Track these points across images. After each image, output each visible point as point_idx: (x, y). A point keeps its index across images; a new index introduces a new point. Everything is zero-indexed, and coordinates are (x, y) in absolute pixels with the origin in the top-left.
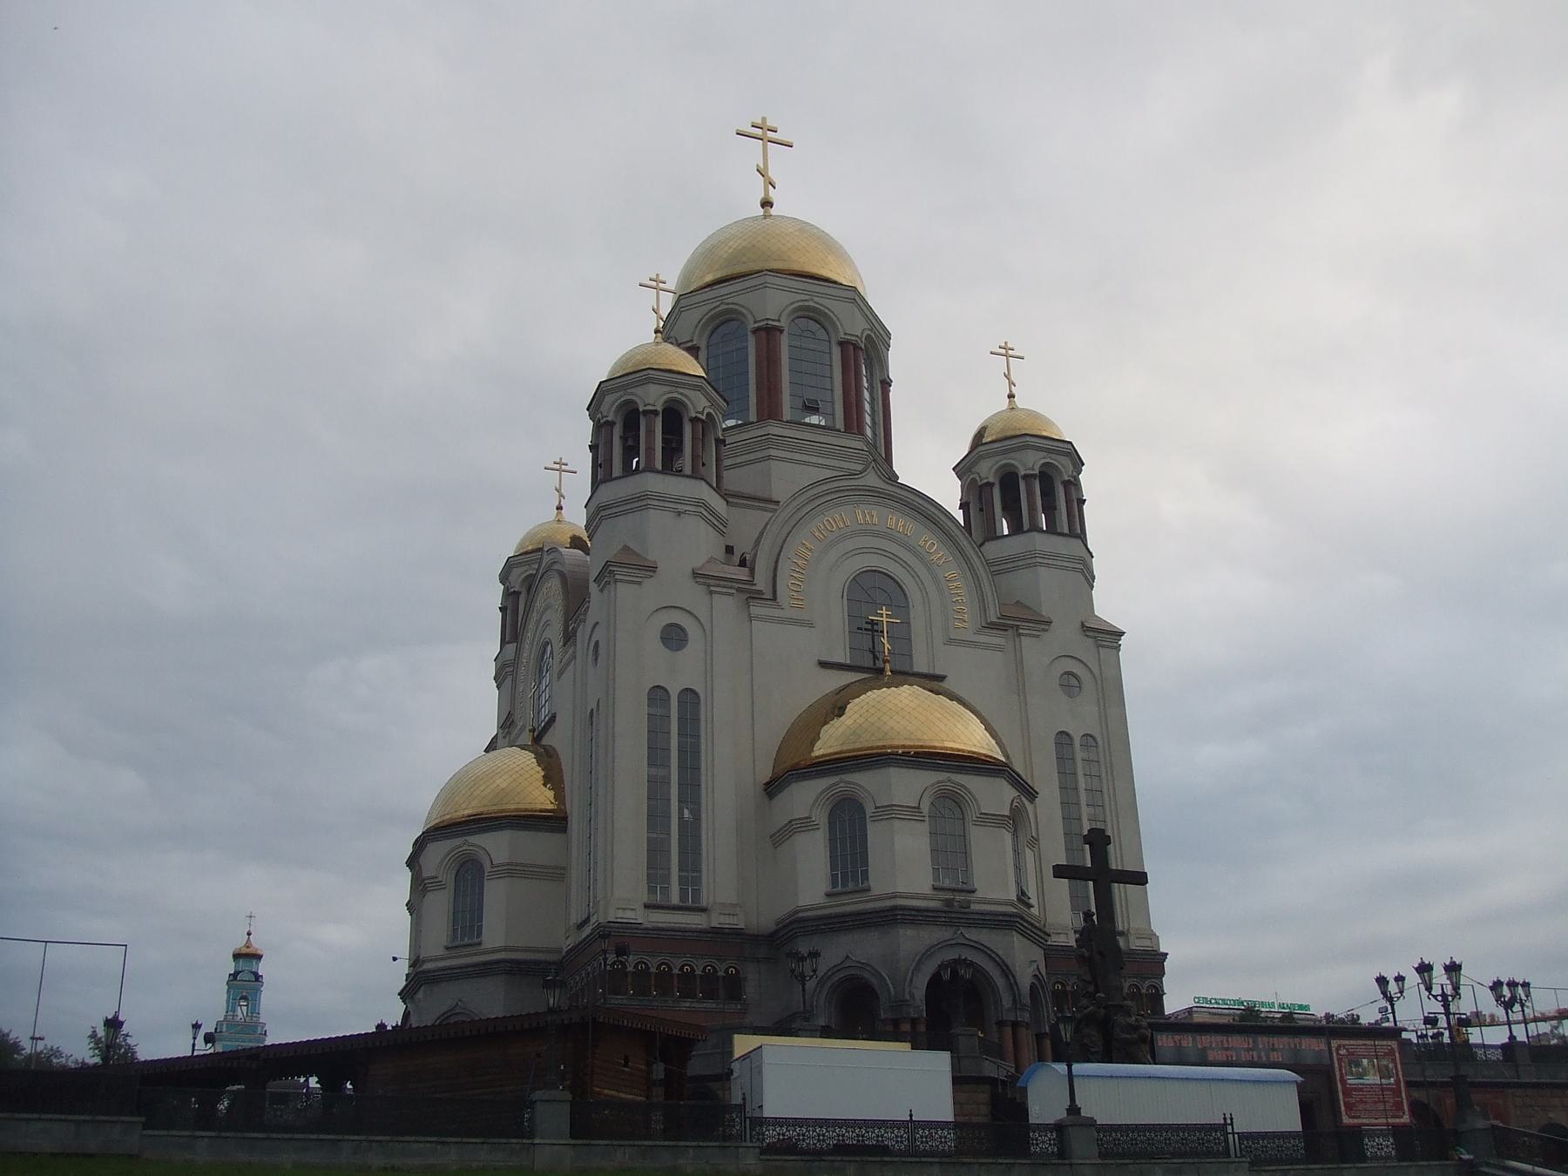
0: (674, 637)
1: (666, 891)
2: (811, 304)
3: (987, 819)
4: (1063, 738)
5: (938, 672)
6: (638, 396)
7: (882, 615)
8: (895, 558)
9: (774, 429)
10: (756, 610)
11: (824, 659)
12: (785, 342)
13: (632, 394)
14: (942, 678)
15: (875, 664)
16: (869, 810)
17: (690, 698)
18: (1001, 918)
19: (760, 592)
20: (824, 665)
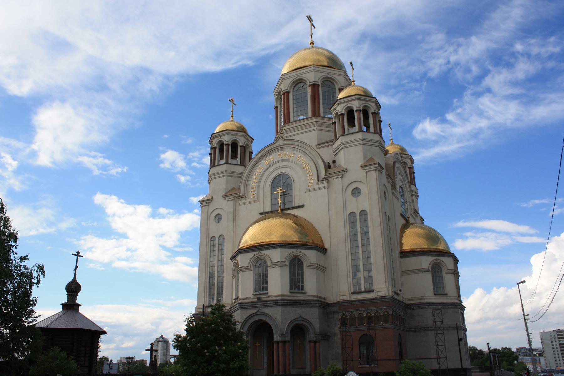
0: (218, 217)
1: (213, 300)
2: (298, 78)
3: (274, 264)
5: (301, 204)
6: (223, 139)
7: (278, 190)
8: (275, 170)
11: (262, 211)
12: (291, 95)
13: (222, 138)
14: (302, 206)
15: (284, 207)
16: (269, 263)
17: (221, 237)
19: (242, 196)
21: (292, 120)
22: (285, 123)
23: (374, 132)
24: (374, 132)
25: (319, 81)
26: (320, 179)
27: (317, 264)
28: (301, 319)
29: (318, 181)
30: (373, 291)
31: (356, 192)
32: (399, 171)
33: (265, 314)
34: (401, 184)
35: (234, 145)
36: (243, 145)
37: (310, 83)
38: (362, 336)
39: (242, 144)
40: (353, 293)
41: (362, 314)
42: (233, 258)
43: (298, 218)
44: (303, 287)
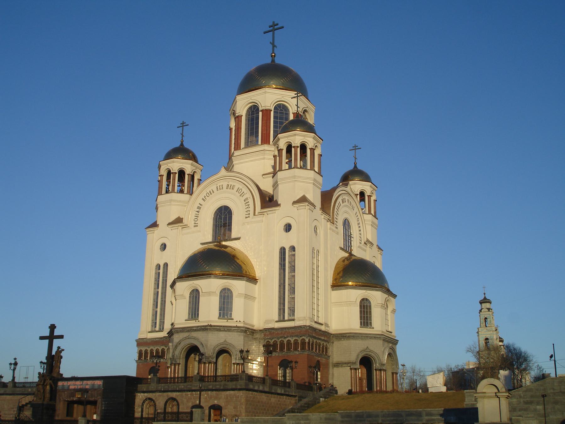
0: (164, 247)
1: (155, 327)
4: (283, 251)
5: (239, 236)
9: (237, 153)
10: (186, 231)
17: (166, 265)
18: (203, 328)
20: (202, 244)
21: (243, 145)
22: (235, 150)
23: (309, 169)
24: (309, 169)
25: (272, 106)
26: (256, 214)
27: (246, 295)
28: (225, 343)
29: (254, 215)
30: (294, 320)
31: (288, 228)
32: (346, 203)
33: (195, 338)
34: (346, 216)
35: (182, 173)
36: (190, 173)
37: (262, 107)
38: (283, 360)
39: (189, 172)
40: (276, 322)
41: (283, 341)
42: (172, 286)
43: (235, 250)
44: (231, 314)
